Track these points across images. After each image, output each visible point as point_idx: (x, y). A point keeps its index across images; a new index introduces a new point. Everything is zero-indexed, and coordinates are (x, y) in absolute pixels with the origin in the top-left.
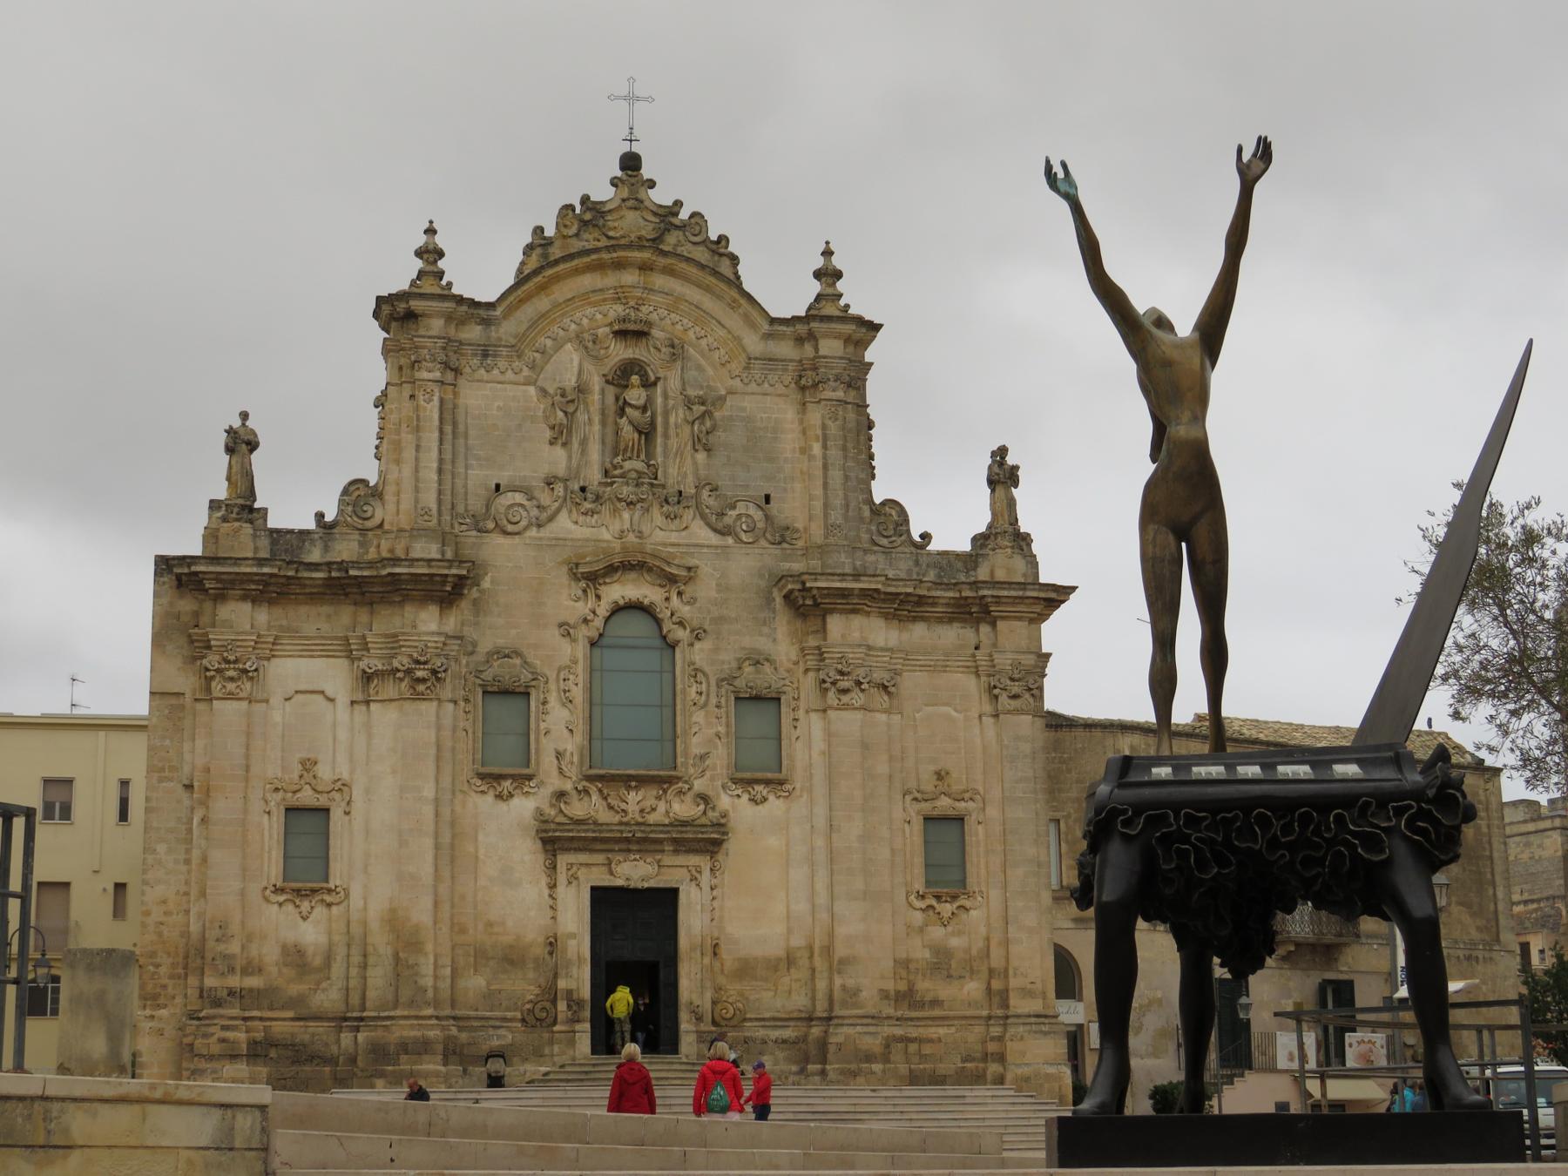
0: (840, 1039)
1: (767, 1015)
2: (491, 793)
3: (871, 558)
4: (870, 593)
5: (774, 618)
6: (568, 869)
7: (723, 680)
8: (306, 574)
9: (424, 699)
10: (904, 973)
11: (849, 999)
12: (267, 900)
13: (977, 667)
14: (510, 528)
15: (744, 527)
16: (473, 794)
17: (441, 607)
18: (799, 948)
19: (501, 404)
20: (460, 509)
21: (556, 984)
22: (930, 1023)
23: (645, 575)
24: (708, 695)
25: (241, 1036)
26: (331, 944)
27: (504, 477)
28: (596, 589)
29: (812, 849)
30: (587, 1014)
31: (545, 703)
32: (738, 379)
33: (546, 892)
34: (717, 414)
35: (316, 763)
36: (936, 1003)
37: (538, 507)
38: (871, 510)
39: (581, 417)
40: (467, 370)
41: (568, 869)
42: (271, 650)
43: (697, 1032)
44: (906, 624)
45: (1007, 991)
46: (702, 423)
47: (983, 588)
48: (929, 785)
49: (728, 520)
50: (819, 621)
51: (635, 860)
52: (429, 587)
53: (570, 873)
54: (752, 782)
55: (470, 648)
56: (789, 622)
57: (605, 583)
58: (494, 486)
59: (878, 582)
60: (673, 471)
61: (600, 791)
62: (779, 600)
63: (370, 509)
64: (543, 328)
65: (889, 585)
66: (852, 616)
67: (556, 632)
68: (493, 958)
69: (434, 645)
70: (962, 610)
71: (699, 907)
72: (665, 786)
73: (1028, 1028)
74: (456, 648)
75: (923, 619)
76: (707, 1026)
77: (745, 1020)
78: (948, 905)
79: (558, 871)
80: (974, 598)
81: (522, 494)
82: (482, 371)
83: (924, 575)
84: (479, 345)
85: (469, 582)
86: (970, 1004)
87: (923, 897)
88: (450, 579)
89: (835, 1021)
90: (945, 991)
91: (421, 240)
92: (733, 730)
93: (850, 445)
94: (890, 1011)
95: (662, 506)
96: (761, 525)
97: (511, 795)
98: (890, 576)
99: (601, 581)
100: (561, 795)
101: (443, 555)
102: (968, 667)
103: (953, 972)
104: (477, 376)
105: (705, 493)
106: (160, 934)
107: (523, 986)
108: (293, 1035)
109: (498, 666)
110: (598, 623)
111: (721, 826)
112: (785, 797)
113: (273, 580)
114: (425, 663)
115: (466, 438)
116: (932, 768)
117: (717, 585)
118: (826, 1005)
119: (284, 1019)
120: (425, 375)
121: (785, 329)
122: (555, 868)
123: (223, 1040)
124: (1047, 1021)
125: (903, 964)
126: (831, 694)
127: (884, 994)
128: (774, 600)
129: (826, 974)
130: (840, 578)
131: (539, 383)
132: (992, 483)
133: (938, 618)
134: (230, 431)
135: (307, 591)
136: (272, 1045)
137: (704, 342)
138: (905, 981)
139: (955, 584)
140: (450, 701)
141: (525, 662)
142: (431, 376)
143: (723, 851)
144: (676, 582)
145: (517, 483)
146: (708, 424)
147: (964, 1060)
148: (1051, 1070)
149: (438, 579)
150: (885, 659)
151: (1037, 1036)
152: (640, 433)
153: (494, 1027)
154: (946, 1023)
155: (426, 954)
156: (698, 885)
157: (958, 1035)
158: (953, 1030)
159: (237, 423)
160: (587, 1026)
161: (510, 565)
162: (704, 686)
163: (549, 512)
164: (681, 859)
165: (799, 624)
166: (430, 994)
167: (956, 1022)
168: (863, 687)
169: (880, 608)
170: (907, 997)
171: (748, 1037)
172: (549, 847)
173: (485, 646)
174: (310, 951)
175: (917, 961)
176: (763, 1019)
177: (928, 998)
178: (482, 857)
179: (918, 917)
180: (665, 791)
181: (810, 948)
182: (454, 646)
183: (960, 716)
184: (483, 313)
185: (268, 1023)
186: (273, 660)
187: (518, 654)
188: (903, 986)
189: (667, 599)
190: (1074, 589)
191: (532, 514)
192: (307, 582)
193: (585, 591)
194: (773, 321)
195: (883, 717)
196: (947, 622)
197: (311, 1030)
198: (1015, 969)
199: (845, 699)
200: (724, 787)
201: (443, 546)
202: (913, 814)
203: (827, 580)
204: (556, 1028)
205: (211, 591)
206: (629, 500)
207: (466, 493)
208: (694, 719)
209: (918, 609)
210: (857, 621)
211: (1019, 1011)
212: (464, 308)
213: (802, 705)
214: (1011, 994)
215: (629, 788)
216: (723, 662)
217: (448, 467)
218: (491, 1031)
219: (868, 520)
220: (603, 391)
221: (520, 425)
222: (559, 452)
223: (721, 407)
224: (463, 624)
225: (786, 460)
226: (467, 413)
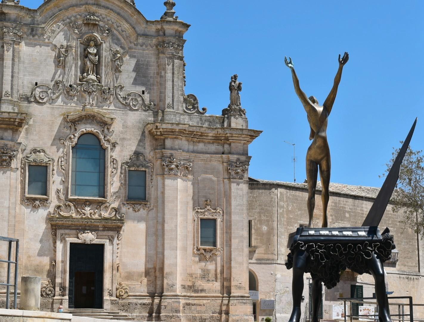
0: (166, 304)
1: (137, 294)
3: (182, 117)
4: (183, 131)
5: (144, 139)
6: (61, 236)
7: (124, 163)
10: (191, 278)
11: (169, 288)
14: (41, 101)
17: (13, 131)
18: (150, 268)
19: (38, 51)
21: (55, 281)
23: (94, 121)
27: (39, 80)
28: (75, 126)
29: (157, 230)
30: (67, 292)
32: (133, 44)
33: (52, 244)
36: (202, 291)
38: (184, 98)
43: (110, 300)
45: (230, 287)
50: (162, 141)
51: (88, 233)
52: (8, 122)
54: (133, 204)
55: (24, 148)
56: (150, 141)
57: (78, 124)
58: (35, 83)
61: (74, 206)
62: (147, 132)
66: (176, 139)
72: (100, 204)
75: (203, 142)
76: (114, 298)
79: (57, 236)
80: (223, 134)
82: (31, 37)
83: (203, 125)
86: (216, 291)
88: (17, 120)
92: (127, 183)
93: (176, 72)
95: (102, 94)
96: (141, 102)
98: (191, 125)
99: (77, 123)
100: (59, 207)
101: (14, 110)
102: (219, 161)
103: (210, 279)
105: (118, 90)
110: (76, 140)
114: (6, 153)
115: (24, 63)
116: (204, 199)
117: (123, 125)
118: (160, 290)
121: (152, 25)
122: (56, 235)
124: (245, 298)
125: (191, 275)
126: (166, 169)
129: (161, 279)
130: (171, 125)
132: (231, 88)
133: (208, 141)
137: (120, 29)
138: (191, 282)
139: (216, 128)
143: (122, 230)
144: (107, 124)
145: (44, 83)
147: (213, 313)
148: (246, 317)
149: (12, 120)
151: (241, 304)
152: (94, 64)
154: (206, 298)
155: (4, 268)
158: (209, 301)
160: (67, 297)
161: (41, 115)
165: (154, 142)
168: (178, 168)
170: (192, 288)
172: (54, 228)
175: (196, 274)
177: (200, 288)
180: (100, 207)
181: (155, 268)
183: (215, 179)
187: (44, 151)
188: (190, 284)
189: (103, 131)
190: (261, 132)
193: (70, 127)
194: (147, 21)
198: (234, 278)
200: (124, 204)
201: (14, 106)
204: (55, 298)
206: (89, 91)
210: (177, 142)
213: (154, 173)
214: (232, 288)
215: (86, 205)
217: (15, 75)
221: (45, 60)
225: (151, 77)
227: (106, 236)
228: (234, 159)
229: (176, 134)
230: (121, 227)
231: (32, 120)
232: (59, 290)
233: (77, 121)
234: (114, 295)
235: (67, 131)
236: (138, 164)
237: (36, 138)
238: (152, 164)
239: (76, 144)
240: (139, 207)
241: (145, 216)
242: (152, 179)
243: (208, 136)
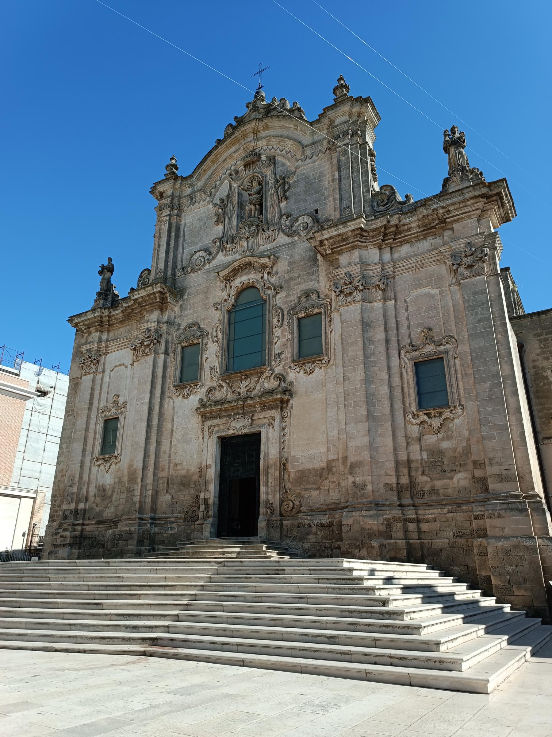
4: (358, 232)
13: (444, 258)
44: (396, 248)
54: (303, 364)
70: (429, 226)
71: (274, 441)
75: (406, 242)
111: (288, 392)
133: (415, 237)
143: (290, 406)
164: (264, 414)
169: (372, 242)
196: (423, 239)
199: (349, 299)
210: (356, 253)
227: (265, 418)
229: (351, 241)
230: (288, 401)
231: (186, 294)
236: (307, 306)
238: (329, 300)
241: (322, 377)
242: (330, 321)
243: (411, 228)
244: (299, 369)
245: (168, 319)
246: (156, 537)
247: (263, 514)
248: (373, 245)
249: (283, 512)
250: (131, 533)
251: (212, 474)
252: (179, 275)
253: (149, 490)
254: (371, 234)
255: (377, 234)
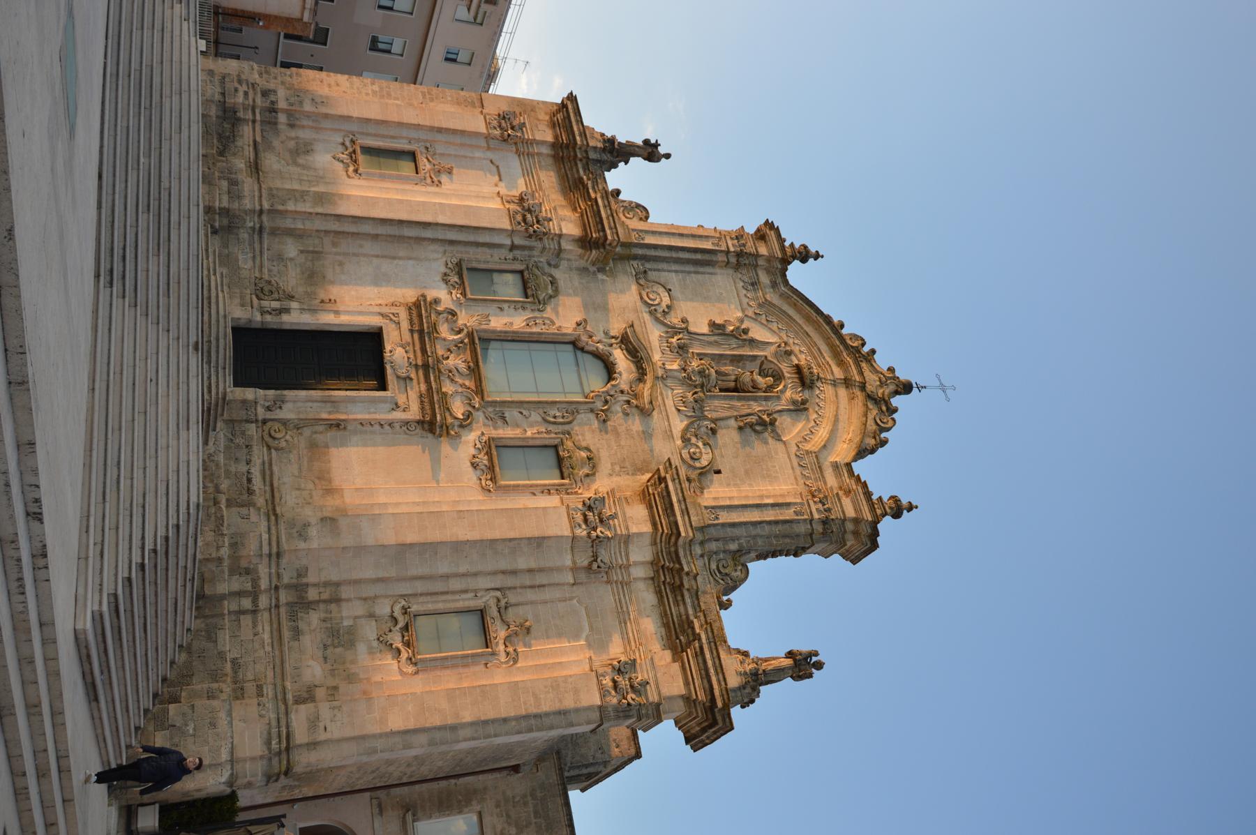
0: (254, 518)
1: (275, 468)
2: (448, 271)
5: (628, 474)
8: (580, 165)
9: (511, 221)
10: (325, 596)
12: (344, 136)
15: (692, 450)
16: (444, 259)
18: (343, 497)
20: (648, 265)
22: (275, 626)
24: (554, 423)
25: (240, 98)
26: (315, 169)
31: (524, 308)
34: (766, 434)
35: (450, 173)
36: (297, 633)
37: (664, 311)
39: (734, 342)
40: (740, 276)
41: (393, 314)
42: (523, 154)
44: (653, 587)
46: (758, 424)
47: (707, 633)
48: (511, 615)
49: (694, 440)
53: (391, 315)
55: (553, 263)
59: (686, 532)
60: (716, 403)
63: (631, 216)
64: (781, 319)
65: (685, 550)
67: (578, 319)
68: (313, 265)
69: (552, 228)
73: (274, 723)
74: (552, 247)
77: (269, 448)
78: (400, 638)
81: (669, 302)
84: (758, 279)
85: (602, 250)
87: (405, 611)
89: (273, 518)
90: (310, 642)
91: (813, 249)
94: (286, 580)
97: (446, 283)
104: (738, 280)
106: (313, 80)
107: (291, 280)
108: (242, 136)
109: (544, 279)
112: (481, 483)
113: (571, 149)
119: (254, 136)
120: (730, 243)
123: (236, 90)
127: (302, 573)
128: (643, 474)
130: (681, 498)
131: (745, 319)
133: (665, 611)
134: (656, 145)
135: (568, 172)
136: (233, 126)
140: (513, 242)
141: (551, 297)
142: (730, 245)
143: (425, 434)
146: (758, 428)
147: (234, 662)
150: (620, 560)
152: (736, 381)
153: (254, 257)
155: (313, 207)
156: (393, 409)
157: (261, 653)
158: (268, 649)
159: (662, 150)
162: (561, 420)
163: (662, 319)
166: (280, 207)
167: (277, 653)
169: (662, 552)
170: (302, 604)
171: (251, 448)
173: (555, 272)
174: (307, 157)
175: (340, 612)
176: (270, 464)
177: (302, 625)
178: (396, 262)
179: (383, 609)
182: (553, 245)
184: (779, 280)
185: (250, 124)
186: (516, 157)
188: (312, 594)
191: (657, 307)
192: (574, 170)
195: (569, 563)
197: (247, 147)
202: (484, 599)
203: (676, 490)
205: (555, 119)
207: (659, 270)
208: (532, 413)
209: (668, 590)
211: (293, 716)
212: (779, 266)
216: (583, 435)
217: (674, 255)
218: (250, 255)
219: (727, 548)
220: (754, 357)
222: (705, 329)
223: (773, 437)
224: (569, 260)
226: (712, 274)
228: (642, 672)
229: (663, 521)
231: (604, 277)
232: (272, 306)
233: (627, 350)
234: (269, 415)
235: (602, 332)
237: (576, 284)
239: (582, 349)
240: (483, 467)
244: (480, 447)
245: (565, 250)
246: (233, 236)
247: (265, 395)
248: (657, 553)
249: (269, 424)
250: (240, 197)
251: (327, 319)
252: (636, 266)
253: (304, 224)
254: (673, 549)
255: (672, 558)
